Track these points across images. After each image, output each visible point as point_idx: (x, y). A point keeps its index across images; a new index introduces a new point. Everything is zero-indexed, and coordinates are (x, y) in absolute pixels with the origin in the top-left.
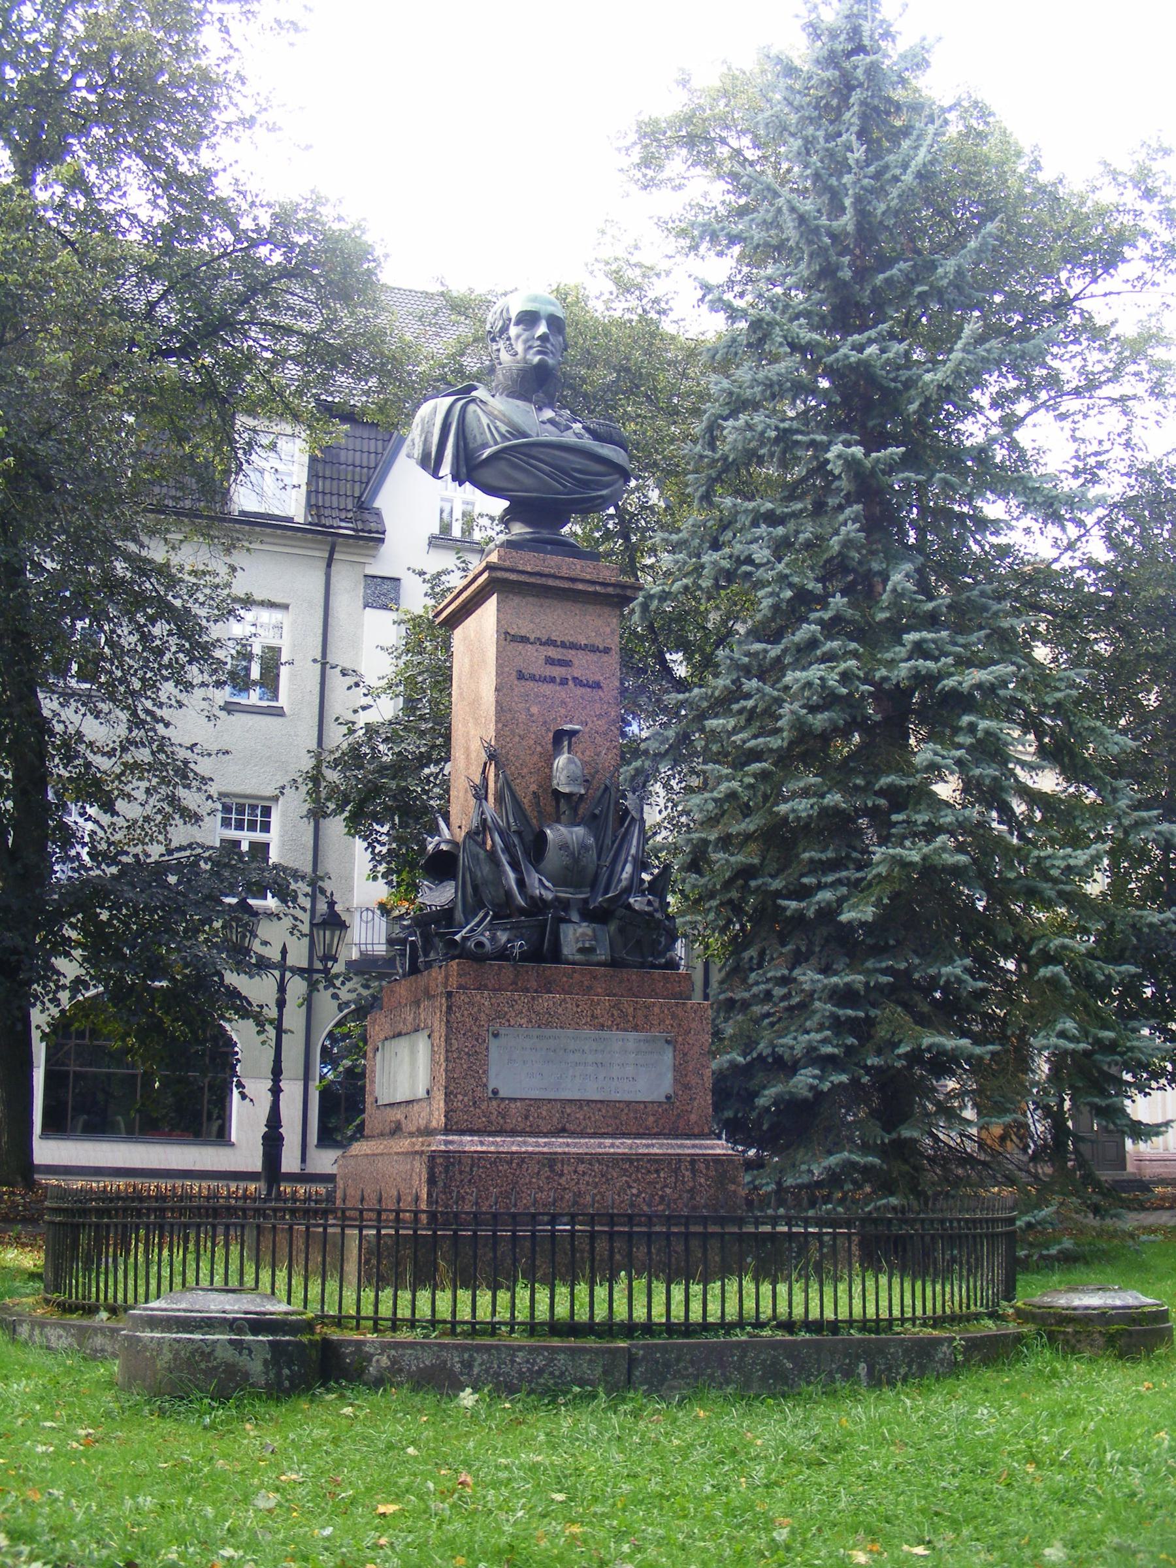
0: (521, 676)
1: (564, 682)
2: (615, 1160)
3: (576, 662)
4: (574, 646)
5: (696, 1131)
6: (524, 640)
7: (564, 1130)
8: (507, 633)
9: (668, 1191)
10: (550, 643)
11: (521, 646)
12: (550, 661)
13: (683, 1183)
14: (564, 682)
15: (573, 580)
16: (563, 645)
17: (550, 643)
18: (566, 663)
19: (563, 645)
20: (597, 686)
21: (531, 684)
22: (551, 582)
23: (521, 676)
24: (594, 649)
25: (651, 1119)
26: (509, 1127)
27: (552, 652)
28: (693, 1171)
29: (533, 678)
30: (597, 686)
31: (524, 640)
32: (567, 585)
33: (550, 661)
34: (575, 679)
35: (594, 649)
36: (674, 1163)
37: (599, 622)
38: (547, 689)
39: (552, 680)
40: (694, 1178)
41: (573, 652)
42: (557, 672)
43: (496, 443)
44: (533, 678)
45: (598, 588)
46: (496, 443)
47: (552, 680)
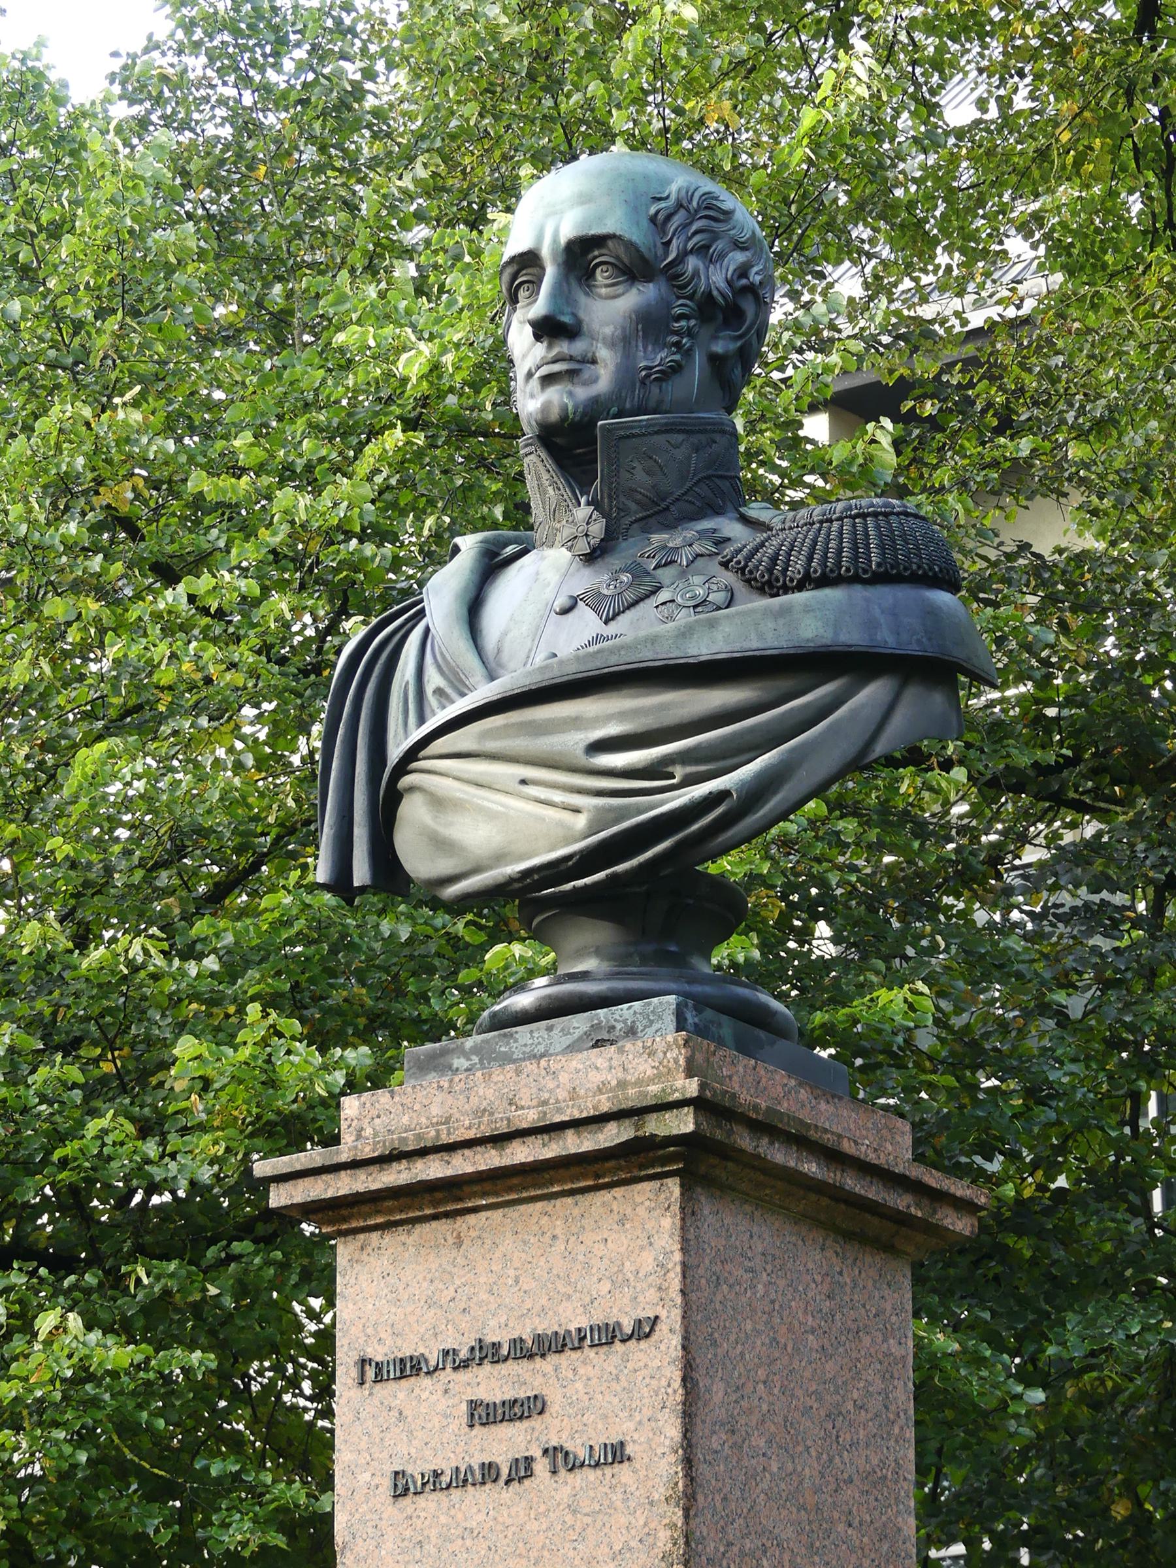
6: (410, 1367)
8: (363, 1362)
12: (483, 1414)
14: (522, 1469)
16: (523, 1351)
19: (523, 1351)
20: (617, 1454)
21: (429, 1503)
24: (608, 1336)
27: (492, 1383)
30: (617, 1454)
31: (410, 1367)
33: (483, 1414)
35: (608, 1336)
39: (489, 1472)
42: (504, 1443)
44: (434, 1481)
47: (489, 1472)
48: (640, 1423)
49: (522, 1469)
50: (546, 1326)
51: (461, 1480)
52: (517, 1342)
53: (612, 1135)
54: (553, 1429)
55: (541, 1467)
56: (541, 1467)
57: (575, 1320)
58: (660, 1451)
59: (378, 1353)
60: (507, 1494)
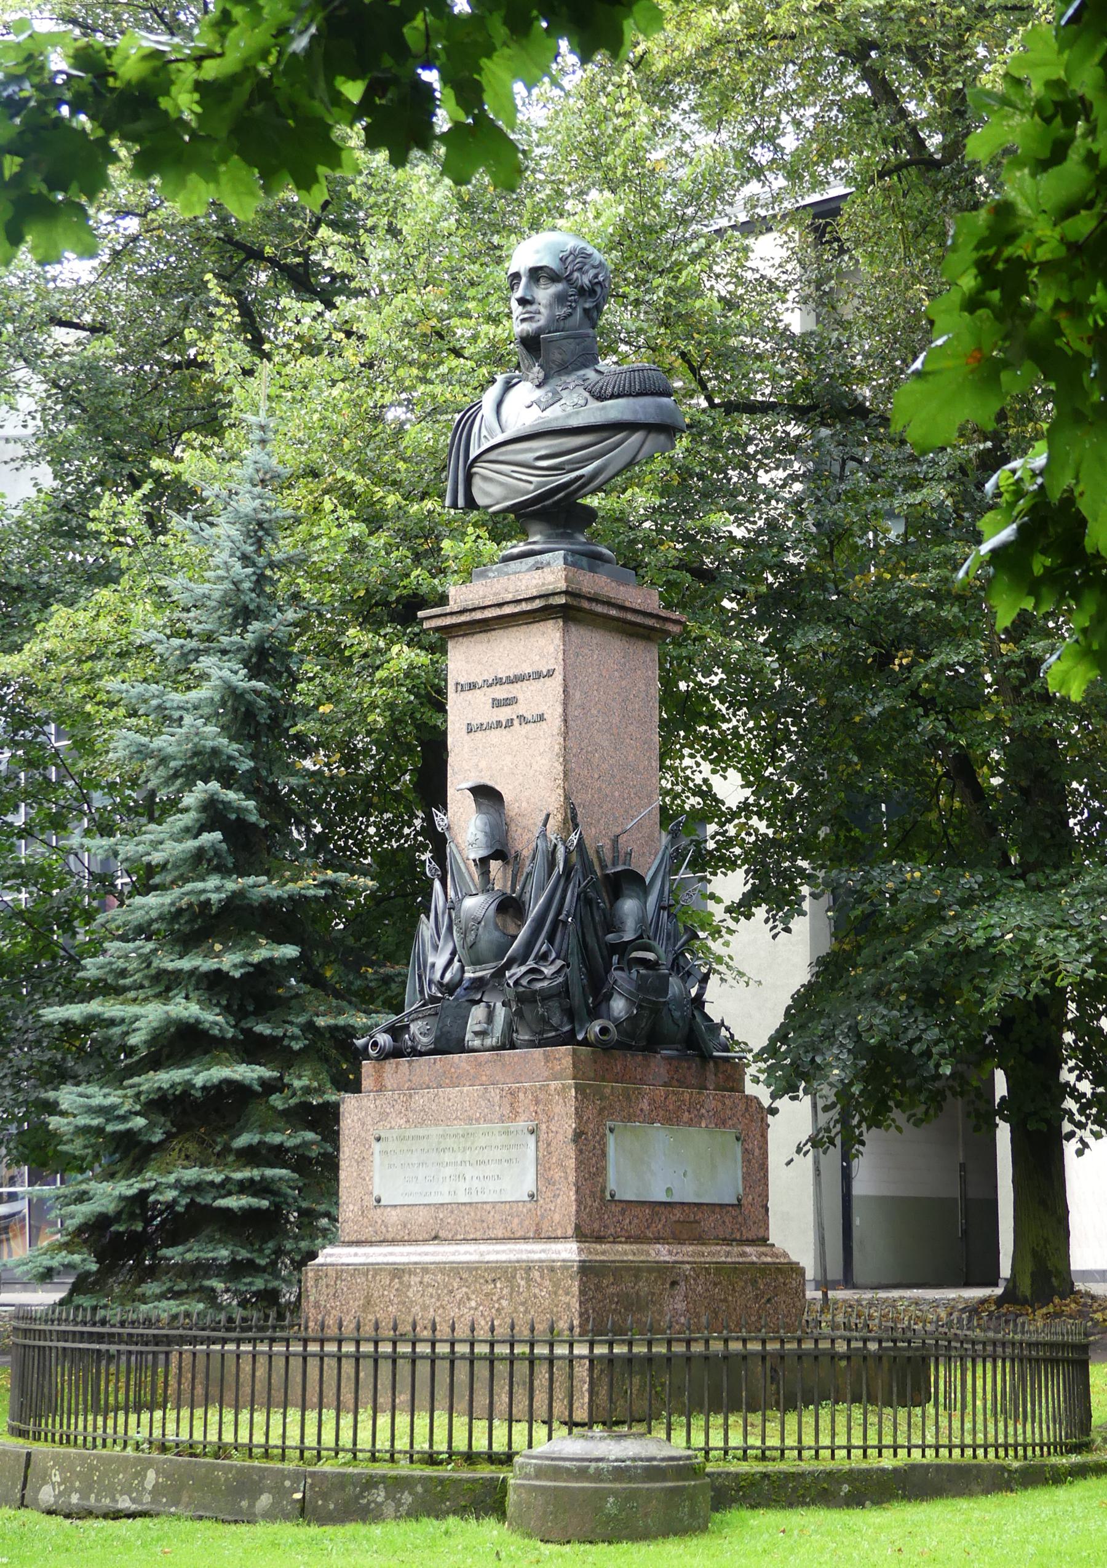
2: (455, 1270)
3: (521, 697)
5: (559, 1233)
6: (472, 686)
7: (436, 1238)
9: (504, 1303)
10: (498, 681)
12: (497, 703)
13: (519, 1294)
14: (510, 723)
15: (500, 605)
17: (498, 681)
20: (541, 718)
21: (479, 734)
22: (478, 615)
24: (538, 675)
25: (516, 1221)
26: (389, 1237)
27: (500, 692)
28: (529, 1280)
30: (541, 718)
31: (472, 686)
32: (496, 612)
33: (497, 703)
35: (538, 675)
36: (505, 1272)
37: (542, 642)
38: (495, 735)
40: (528, 1287)
42: (504, 713)
44: (480, 727)
47: (499, 724)
49: (510, 723)
50: (518, 672)
51: (490, 727)
53: (538, 604)
54: (521, 709)
57: (527, 669)
60: (505, 732)
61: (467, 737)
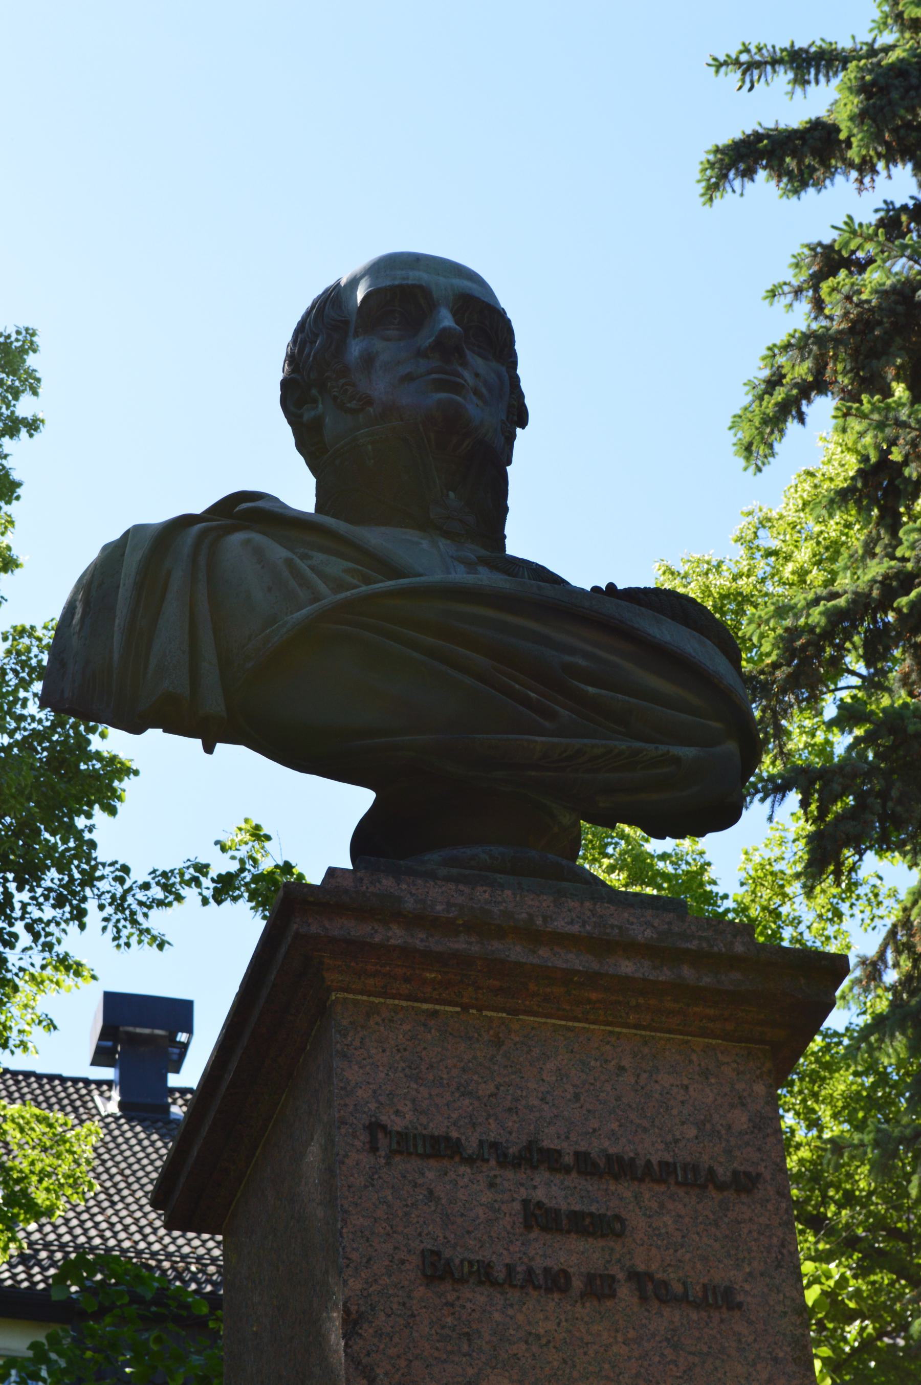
0: (437, 1270)
1: (599, 1287)
4: (620, 1168)
6: (442, 1148)
8: (375, 1128)
10: (536, 1157)
11: (431, 1172)
12: (539, 1218)
14: (599, 1287)
16: (585, 1165)
17: (536, 1157)
18: (602, 1226)
19: (585, 1165)
23: (437, 1270)
27: (551, 1190)
29: (483, 1274)
31: (442, 1148)
33: (539, 1218)
34: (638, 1278)
39: (556, 1282)
41: (625, 1189)
42: (574, 1254)
43: (316, 598)
44: (483, 1274)
45: (687, 972)
46: (316, 598)
47: (556, 1282)
48: (750, 1274)
52: (582, 1158)
55: (625, 1291)
56: (625, 1291)
57: (652, 1150)
58: (780, 1308)
59: (398, 1124)
61: (421, 1291)
